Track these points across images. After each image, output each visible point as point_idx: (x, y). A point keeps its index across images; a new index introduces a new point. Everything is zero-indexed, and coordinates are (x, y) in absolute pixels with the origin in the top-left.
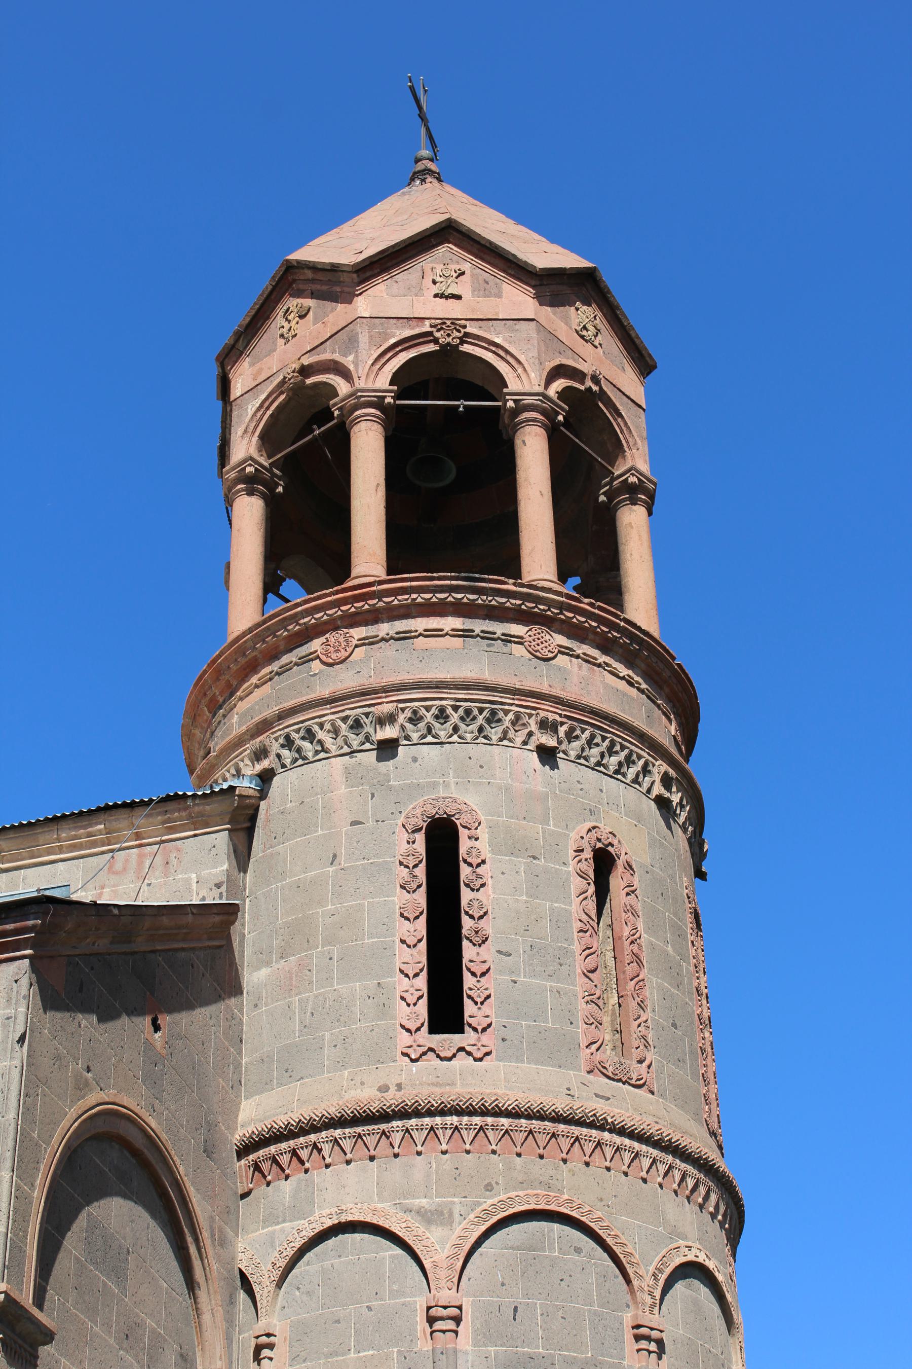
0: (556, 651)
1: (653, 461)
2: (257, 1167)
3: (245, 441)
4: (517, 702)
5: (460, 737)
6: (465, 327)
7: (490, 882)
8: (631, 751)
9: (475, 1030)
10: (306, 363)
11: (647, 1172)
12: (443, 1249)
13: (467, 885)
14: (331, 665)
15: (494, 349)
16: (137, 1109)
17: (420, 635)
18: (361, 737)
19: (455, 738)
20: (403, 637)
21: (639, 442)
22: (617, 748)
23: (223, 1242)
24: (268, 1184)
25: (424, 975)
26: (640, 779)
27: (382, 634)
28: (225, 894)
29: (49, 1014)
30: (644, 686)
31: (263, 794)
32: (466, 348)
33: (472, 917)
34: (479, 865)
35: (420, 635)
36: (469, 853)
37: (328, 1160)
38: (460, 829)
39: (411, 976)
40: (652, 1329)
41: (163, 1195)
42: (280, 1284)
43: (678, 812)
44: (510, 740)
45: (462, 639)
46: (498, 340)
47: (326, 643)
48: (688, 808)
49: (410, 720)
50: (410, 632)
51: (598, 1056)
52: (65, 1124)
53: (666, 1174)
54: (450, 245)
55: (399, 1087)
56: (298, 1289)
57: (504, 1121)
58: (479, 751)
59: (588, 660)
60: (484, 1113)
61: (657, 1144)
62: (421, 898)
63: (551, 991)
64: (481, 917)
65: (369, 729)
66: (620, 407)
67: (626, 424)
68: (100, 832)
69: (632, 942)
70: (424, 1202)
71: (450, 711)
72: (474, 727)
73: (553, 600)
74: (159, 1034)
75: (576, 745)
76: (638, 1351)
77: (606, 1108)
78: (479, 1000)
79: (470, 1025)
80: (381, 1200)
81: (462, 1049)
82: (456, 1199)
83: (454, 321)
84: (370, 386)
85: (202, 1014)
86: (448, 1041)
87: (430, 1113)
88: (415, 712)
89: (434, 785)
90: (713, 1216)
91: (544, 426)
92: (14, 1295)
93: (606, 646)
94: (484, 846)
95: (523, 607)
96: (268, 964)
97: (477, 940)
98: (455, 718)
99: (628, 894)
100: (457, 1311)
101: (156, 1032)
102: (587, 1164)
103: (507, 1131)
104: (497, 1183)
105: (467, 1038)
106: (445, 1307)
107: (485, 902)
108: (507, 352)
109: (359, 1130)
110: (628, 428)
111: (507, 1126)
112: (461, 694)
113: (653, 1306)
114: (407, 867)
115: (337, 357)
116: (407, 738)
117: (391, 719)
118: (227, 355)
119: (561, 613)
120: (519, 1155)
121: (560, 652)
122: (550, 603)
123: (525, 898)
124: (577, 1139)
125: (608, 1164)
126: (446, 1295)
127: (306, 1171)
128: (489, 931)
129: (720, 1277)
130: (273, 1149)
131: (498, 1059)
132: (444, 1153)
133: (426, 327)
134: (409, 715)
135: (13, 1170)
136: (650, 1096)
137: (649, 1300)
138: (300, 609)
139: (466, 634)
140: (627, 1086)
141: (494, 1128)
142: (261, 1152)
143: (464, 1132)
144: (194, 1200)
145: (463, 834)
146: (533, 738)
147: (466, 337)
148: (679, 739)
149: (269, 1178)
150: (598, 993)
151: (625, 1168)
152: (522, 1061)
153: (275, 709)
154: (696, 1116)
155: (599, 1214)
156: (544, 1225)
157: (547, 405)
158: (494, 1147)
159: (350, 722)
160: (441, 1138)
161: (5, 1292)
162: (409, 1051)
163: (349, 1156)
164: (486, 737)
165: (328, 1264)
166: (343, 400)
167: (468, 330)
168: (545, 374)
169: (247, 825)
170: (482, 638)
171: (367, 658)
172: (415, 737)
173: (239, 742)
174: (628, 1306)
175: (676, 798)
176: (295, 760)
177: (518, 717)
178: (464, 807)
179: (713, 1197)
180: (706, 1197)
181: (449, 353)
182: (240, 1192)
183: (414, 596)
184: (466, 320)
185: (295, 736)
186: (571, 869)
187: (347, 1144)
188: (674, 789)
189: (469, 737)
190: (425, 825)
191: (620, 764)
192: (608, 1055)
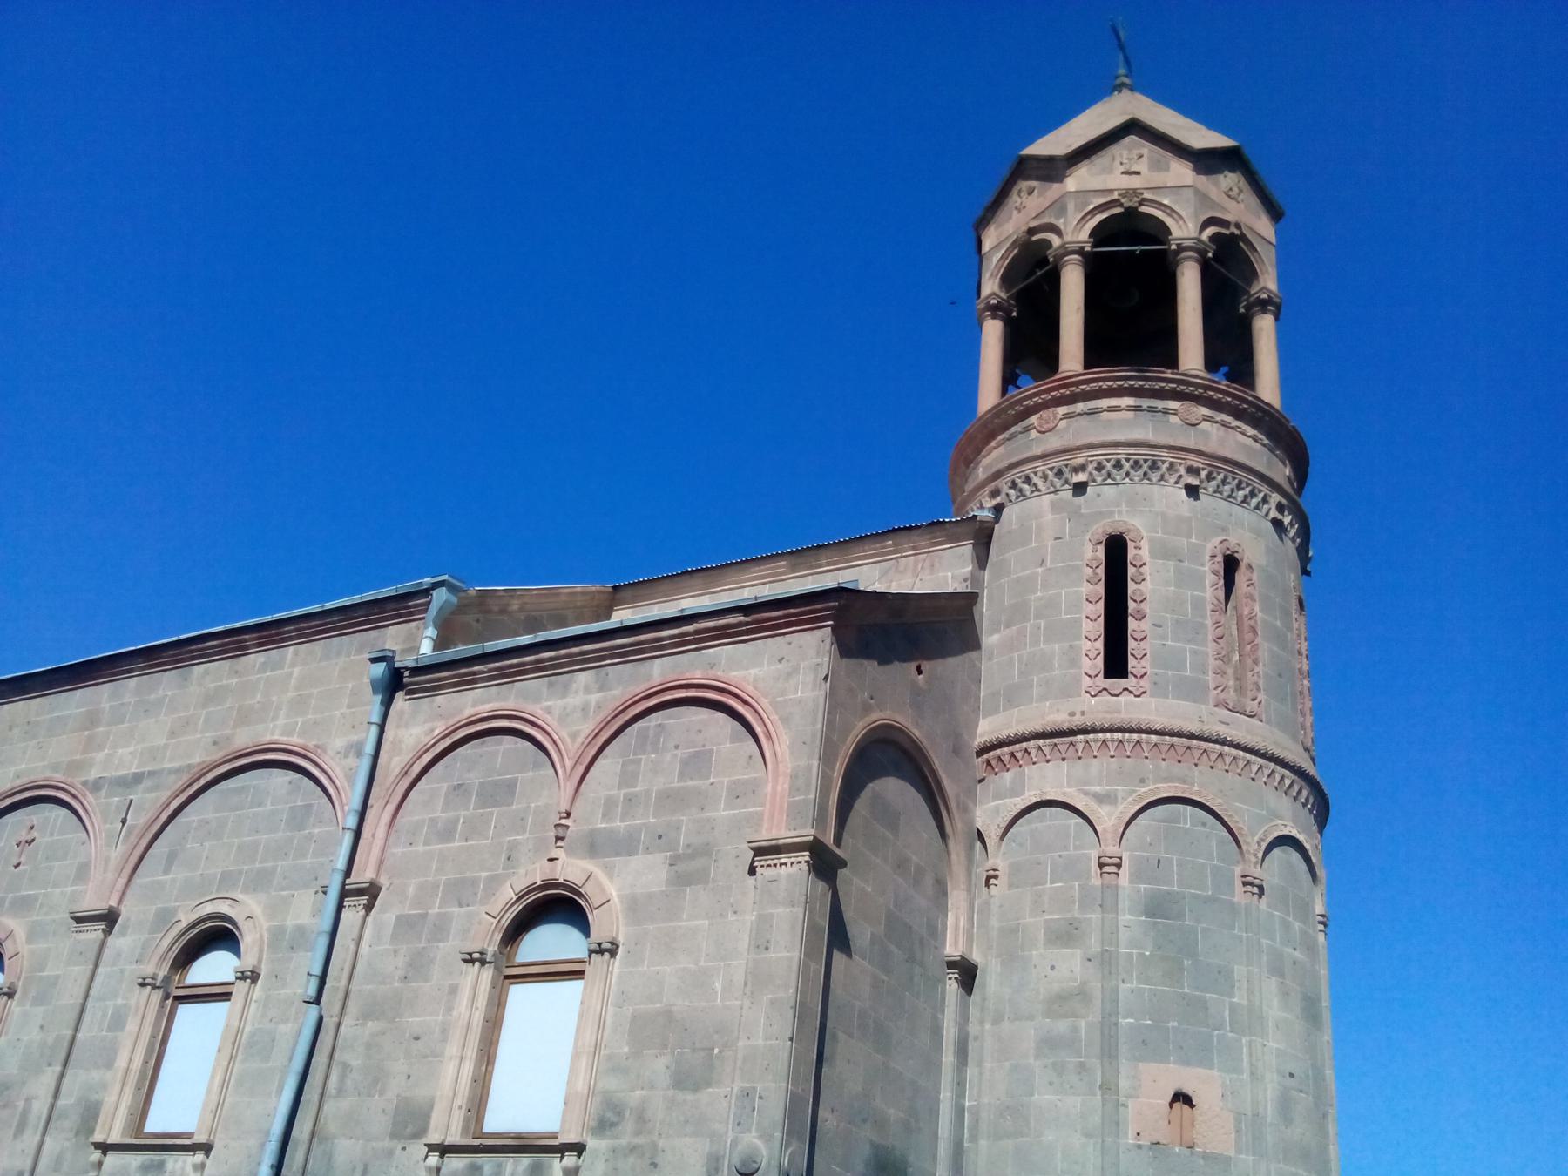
0: (1201, 419)
1: (1281, 280)
2: (988, 763)
3: (991, 282)
4: (1171, 455)
5: (1131, 480)
6: (1142, 194)
7: (1148, 578)
8: (1254, 488)
9: (1136, 676)
10: (1032, 226)
11: (1256, 774)
12: (1110, 819)
13: (1132, 580)
14: (1044, 433)
15: (1163, 208)
16: (906, 724)
17: (1105, 410)
18: (1062, 481)
19: (1127, 480)
20: (1093, 412)
21: (1270, 269)
22: (1244, 485)
23: (965, 810)
24: (996, 774)
25: (1101, 640)
26: (1261, 505)
27: (1078, 411)
28: (969, 586)
29: (845, 660)
30: (1266, 441)
31: (997, 519)
32: (1143, 209)
33: (1135, 601)
34: (1141, 566)
35: (1105, 410)
36: (1134, 558)
37: (1035, 760)
38: (1128, 541)
39: (1092, 640)
40: (1255, 878)
41: (924, 778)
42: (1002, 837)
43: (1289, 529)
44: (1166, 481)
45: (1133, 413)
46: (1166, 202)
47: (1041, 418)
48: (1296, 526)
49: (1096, 469)
50: (1097, 408)
51: (1223, 696)
52: (855, 732)
53: (1269, 776)
54: (1133, 137)
55: (1083, 713)
56: (1014, 841)
57: (1153, 737)
58: (1143, 488)
59: (1225, 425)
60: (1140, 731)
61: (1264, 756)
62: (1100, 589)
63: (1190, 652)
64: (1141, 601)
65: (1067, 475)
66: (1255, 244)
67: (1260, 257)
68: (890, 546)
69: (1250, 619)
70: (1098, 789)
71: (1124, 462)
72: (1140, 472)
73: (1199, 383)
74: (921, 676)
75: (1213, 483)
76: (1245, 892)
77: (1227, 731)
78: (1139, 657)
79: (1132, 673)
80: (1069, 786)
81: (1126, 689)
82: (1119, 788)
83: (1135, 190)
84: (1075, 239)
85: (952, 661)
86: (1117, 684)
87: (1103, 731)
88: (1099, 463)
89: (1112, 513)
90: (1304, 805)
91: (1197, 261)
92: (820, 837)
93: (1238, 414)
94: (1145, 553)
95: (1178, 389)
96: (997, 631)
97: (1138, 616)
98: (1127, 466)
99: (1248, 586)
100: (1118, 860)
101: (919, 674)
102: (1212, 767)
103: (1156, 745)
104: (1148, 778)
105: (1129, 682)
106: (1110, 858)
107: (1145, 591)
108: (1173, 210)
109: (1056, 740)
110: (1263, 261)
111: (1137, 739)
112: (1132, 450)
113: (1256, 863)
114: (1091, 568)
115: (1053, 221)
116: (1094, 481)
117: (1082, 468)
118: (981, 222)
119: (1205, 392)
120: (1164, 760)
122: (1197, 386)
123: (1172, 588)
124: (1205, 751)
125: (1227, 768)
126: (1111, 849)
127: (1020, 766)
128: (1147, 611)
129: (1308, 846)
130: (999, 751)
131: (1151, 696)
132: (1112, 757)
133: (1115, 196)
134: (1095, 465)
135: (820, 760)
136: (1260, 723)
137: (1253, 859)
138: (1023, 395)
139: (1137, 409)
140: (1242, 716)
141: (1147, 742)
142: (992, 753)
143: (1126, 745)
144: (945, 783)
145: (1131, 545)
146: (1182, 479)
148: (1292, 477)
149: (996, 770)
150: (1224, 653)
151: (1239, 771)
152: (1168, 698)
153: (1006, 463)
154: (1294, 738)
155: (1220, 801)
156: (1181, 806)
157: (1201, 246)
158: (1146, 754)
159: (1055, 471)
160: (1110, 747)
161: (814, 835)
162: (1088, 689)
163: (1048, 757)
164: (1149, 479)
165: (1034, 826)
166: (1055, 250)
167: (1147, 195)
169: (985, 540)
170: (1149, 411)
171: (1068, 427)
172: (1099, 480)
173: (983, 485)
174: (1238, 862)
175: (1287, 520)
176: (1018, 497)
177: (1172, 464)
178: (1132, 527)
179: (1305, 793)
180: (1300, 792)
181: (1131, 213)
182: (979, 778)
183: (1101, 384)
185: (1018, 481)
186: (1207, 568)
187: (1047, 750)
188: (1286, 513)
189: (1136, 479)
190: (1105, 539)
191: (1246, 496)
192: (1231, 696)
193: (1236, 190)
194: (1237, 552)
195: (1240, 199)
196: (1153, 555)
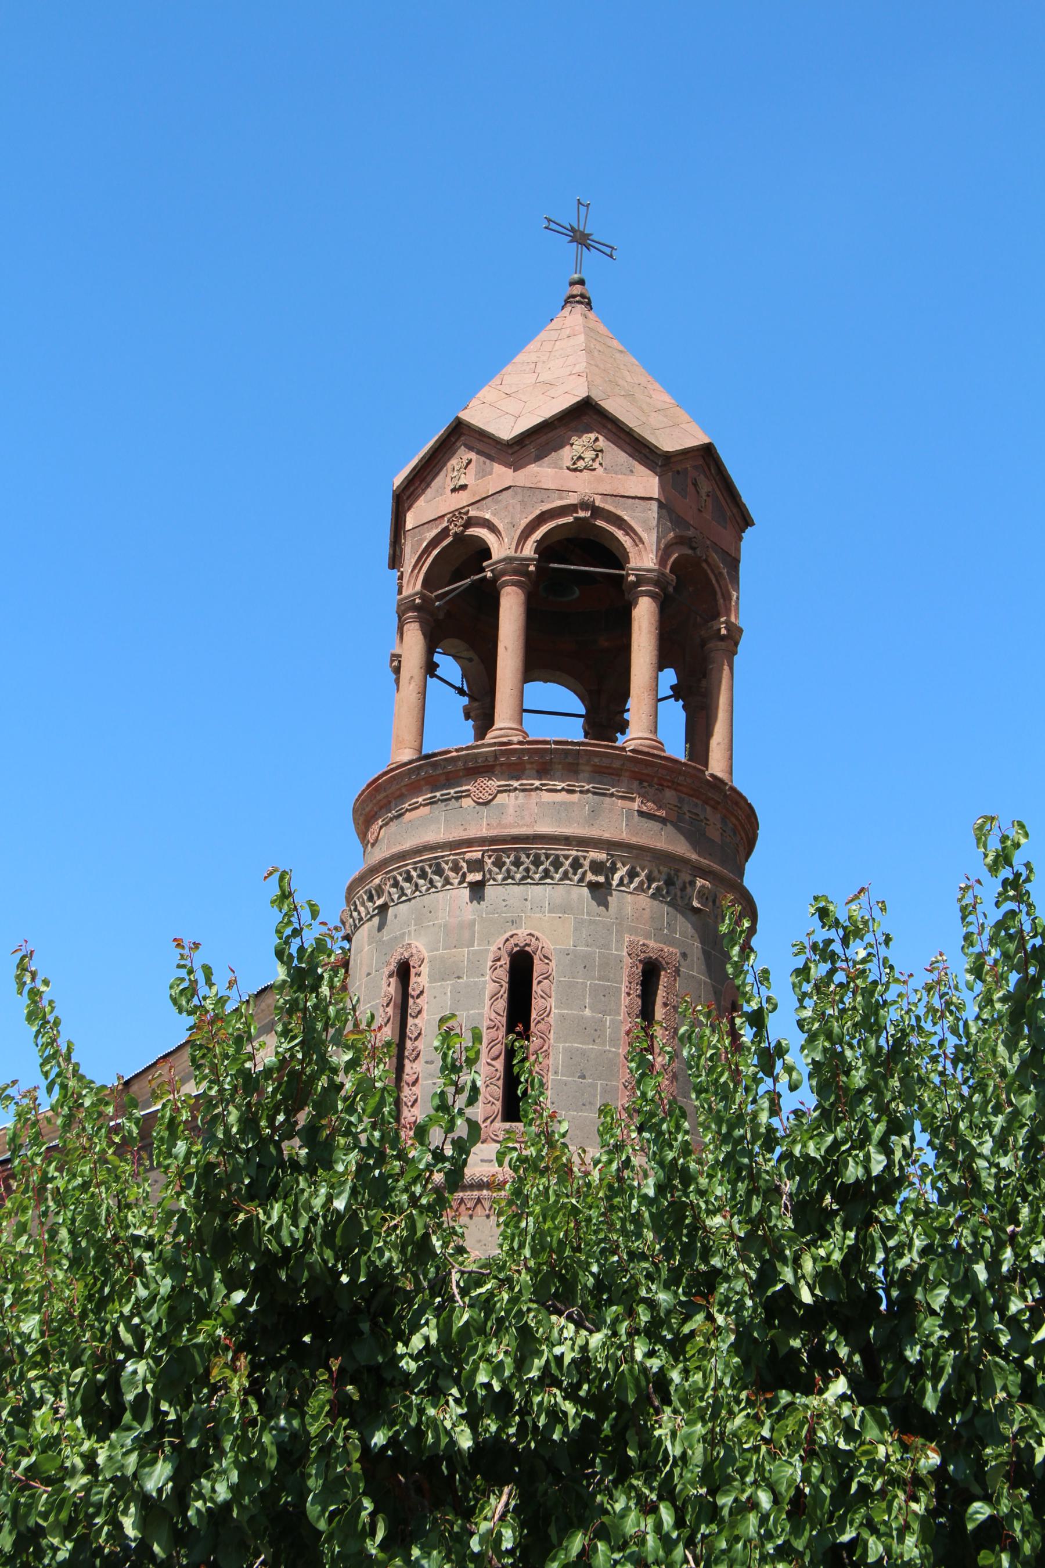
7: (425, 1007)
8: (557, 857)
22: (543, 858)
66: (619, 512)
91: (514, 584)
107: (420, 1025)
121: (499, 792)
133: (445, 524)
139: (432, 803)
145: (413, 971)
147: (470, 523)
167: (472, 513)
168: (519, 532)
178: (414, 951)
181: (460, 539)
184: (468, 506)
186: (488, 978)
193: (589, 455)
194: (526, 945)
195: (596, 465)
196: (432, 979)
